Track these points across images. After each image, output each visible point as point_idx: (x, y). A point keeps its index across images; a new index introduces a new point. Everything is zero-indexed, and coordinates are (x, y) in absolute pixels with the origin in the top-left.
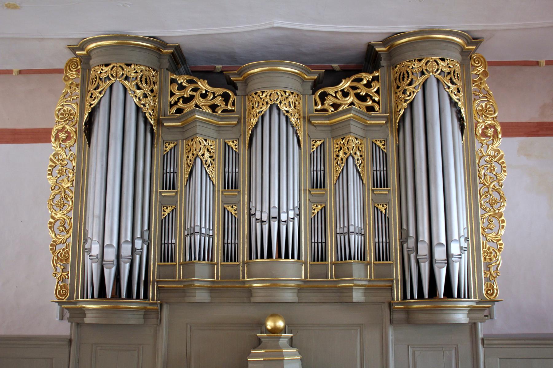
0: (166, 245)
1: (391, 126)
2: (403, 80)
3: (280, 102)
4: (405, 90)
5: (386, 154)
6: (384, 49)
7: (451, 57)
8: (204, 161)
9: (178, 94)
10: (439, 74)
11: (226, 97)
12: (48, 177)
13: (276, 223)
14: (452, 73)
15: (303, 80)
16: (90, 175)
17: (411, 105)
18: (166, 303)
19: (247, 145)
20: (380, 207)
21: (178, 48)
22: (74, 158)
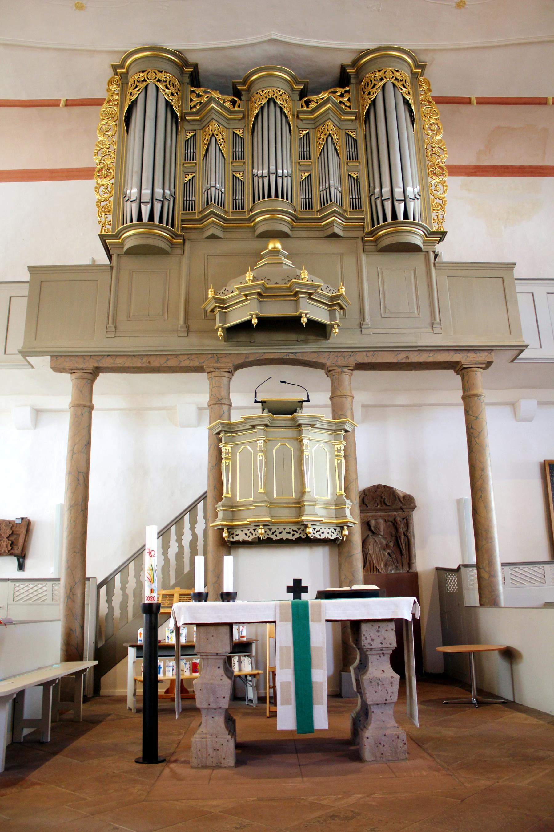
0: (188, 202)
1: (360, 122)
2: (368, 86)
3: (276, 97)
4: (370, 92)
5: (356, 140)
6: (354, 71)
7: (403, 70)
8: (218, 139)
9: (196, 100)
10: (395, 80)
11: (233, 103)
12: (94, 158)
13: (274, 176)
14: (404, 81)
15: (293, 89)
16: (128, 152)
17: (374, 101)
18: (188, 239)
19: (250, 134)
20: (353, 175)
21: (196, 66)
22: (116, 143)
